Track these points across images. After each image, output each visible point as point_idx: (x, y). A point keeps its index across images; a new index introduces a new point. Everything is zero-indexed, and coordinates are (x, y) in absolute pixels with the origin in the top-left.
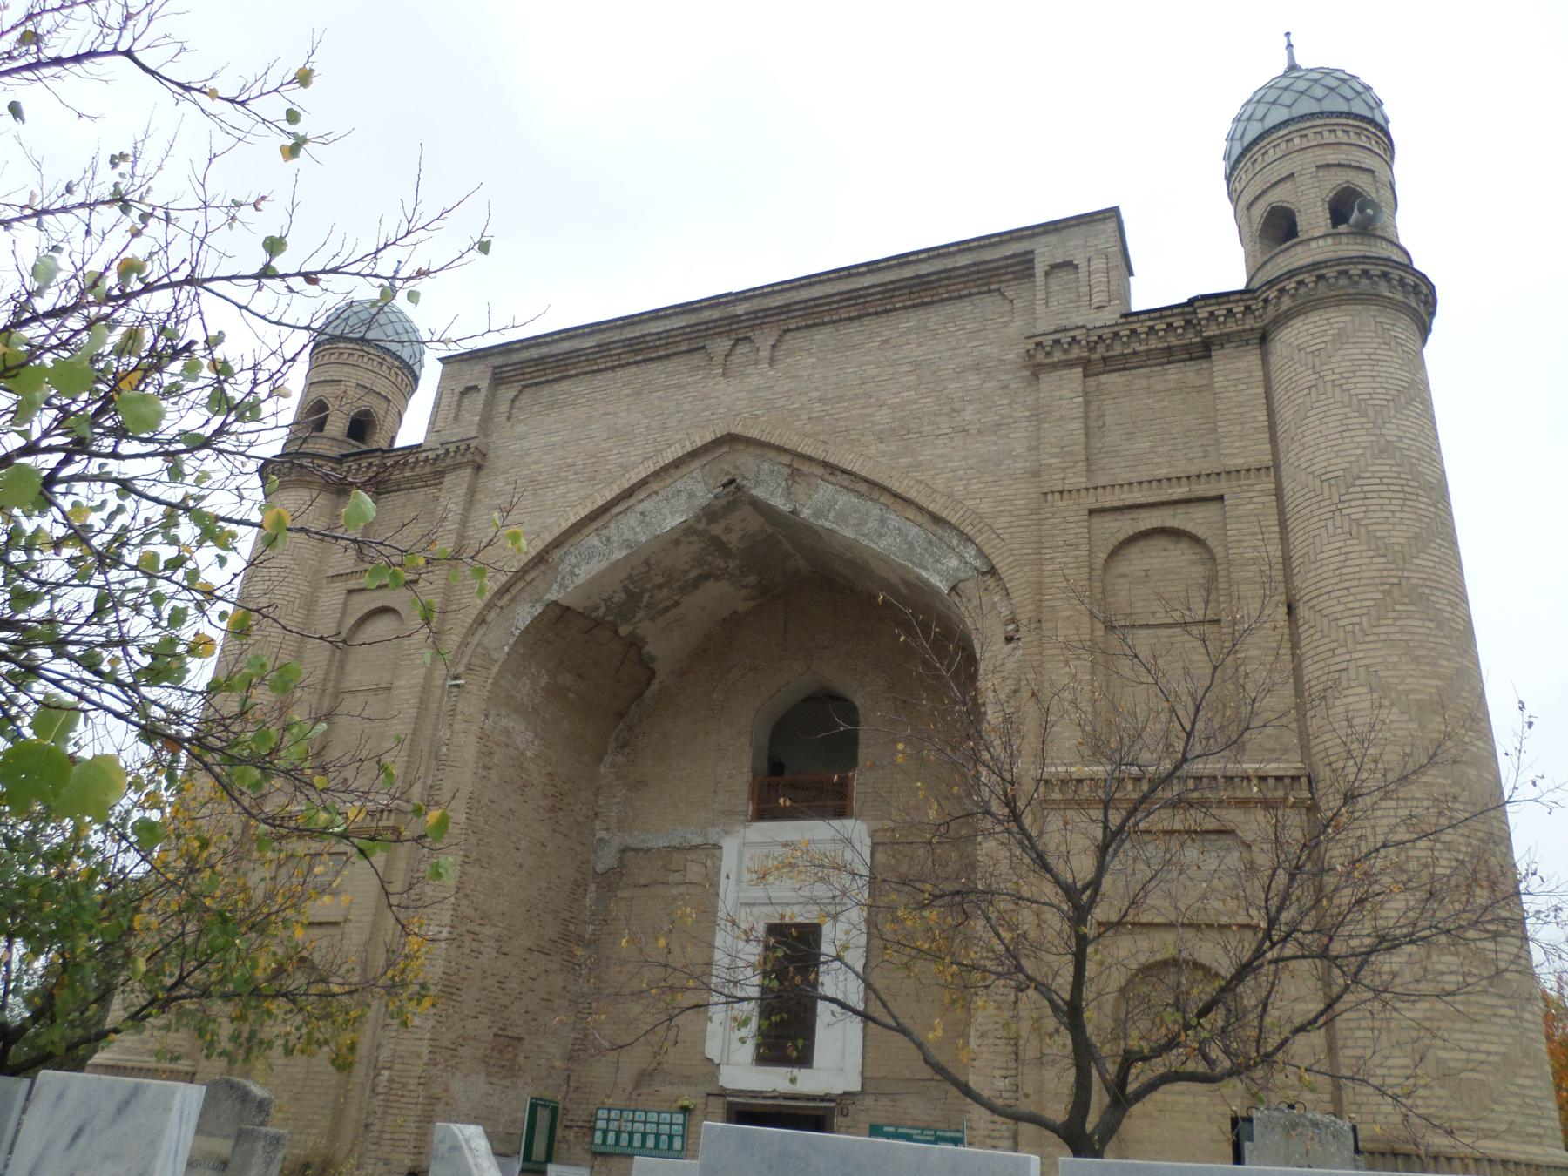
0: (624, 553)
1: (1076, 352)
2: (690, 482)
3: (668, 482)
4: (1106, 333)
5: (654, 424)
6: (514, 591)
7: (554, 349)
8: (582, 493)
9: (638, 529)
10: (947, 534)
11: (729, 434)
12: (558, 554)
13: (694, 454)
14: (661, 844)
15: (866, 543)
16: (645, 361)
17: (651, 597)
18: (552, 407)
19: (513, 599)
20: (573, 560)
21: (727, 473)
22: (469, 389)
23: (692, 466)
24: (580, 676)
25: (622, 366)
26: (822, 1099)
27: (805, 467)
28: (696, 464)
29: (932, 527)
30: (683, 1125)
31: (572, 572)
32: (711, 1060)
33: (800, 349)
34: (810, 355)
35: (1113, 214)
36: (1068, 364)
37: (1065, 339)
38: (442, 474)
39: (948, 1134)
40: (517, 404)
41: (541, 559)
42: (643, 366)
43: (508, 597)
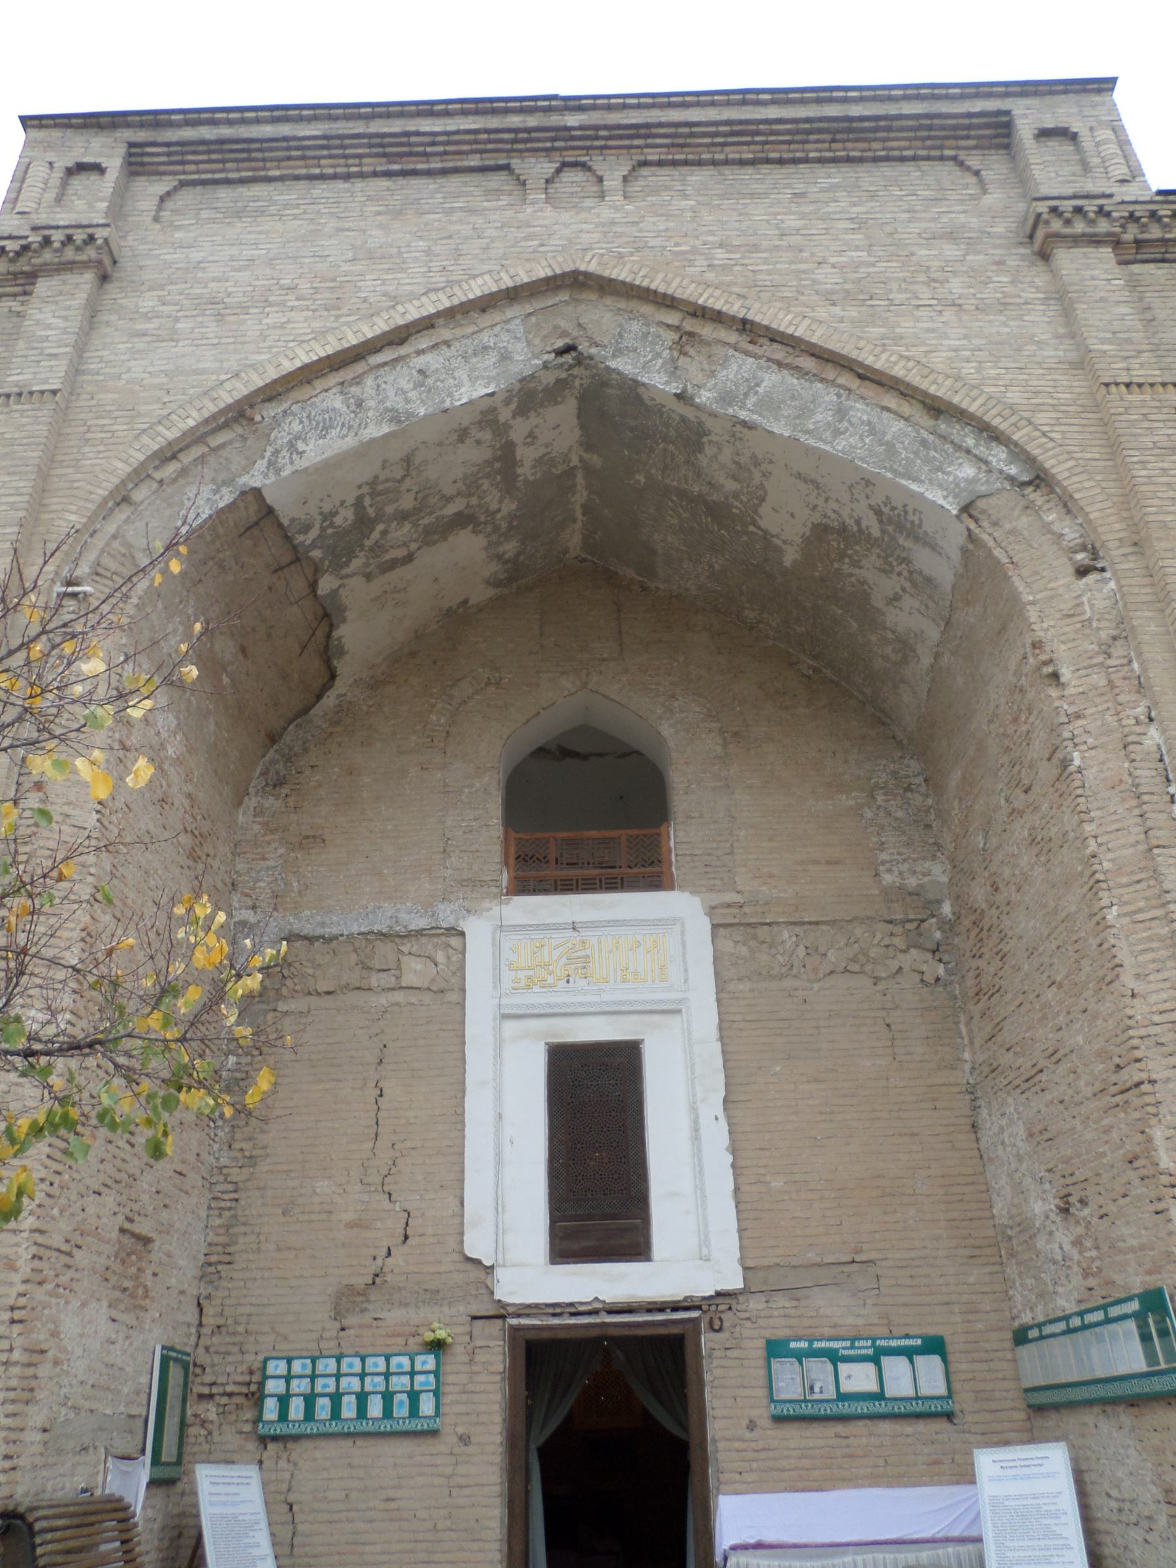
0: (386, 429)
1: (1103, 226)
2: (505, 337)
3: (469, 330)
4: (1140, 210)
5: (437, 249)
6: (186, 458)
7: (245, 132)
8: (317, 324)
9: (413, 395)
10: (956, 431)
11: (575, 273)
12: (271, 410)
13: (513, 295)
14: (355, 929)
15: (811, 442)
16: (404, 173)
17: (384, 533)
18: (238, 214)
19: (184, 472)
20: (296, 427)
21: (564, 334)
22: (81, 168)
23: (509, 313)
24: (243, 650)
25: (362, 176)
26: (676, 1307)
27: (707, 331)
28: (515, 311)
29: (928, 422)
30: (436, 1373)
31: (291, 446)
32: (477, 1262)
33: (667, 188)
34: (685, 196)
35: (1105, 85)
36: (1095, 241)
37: (1090, 207)
38: (32, 276)
39: (894, 1343)
40: (169, 204)
41: (240, 414)
42: (401, 181)
43: (171, 469)
